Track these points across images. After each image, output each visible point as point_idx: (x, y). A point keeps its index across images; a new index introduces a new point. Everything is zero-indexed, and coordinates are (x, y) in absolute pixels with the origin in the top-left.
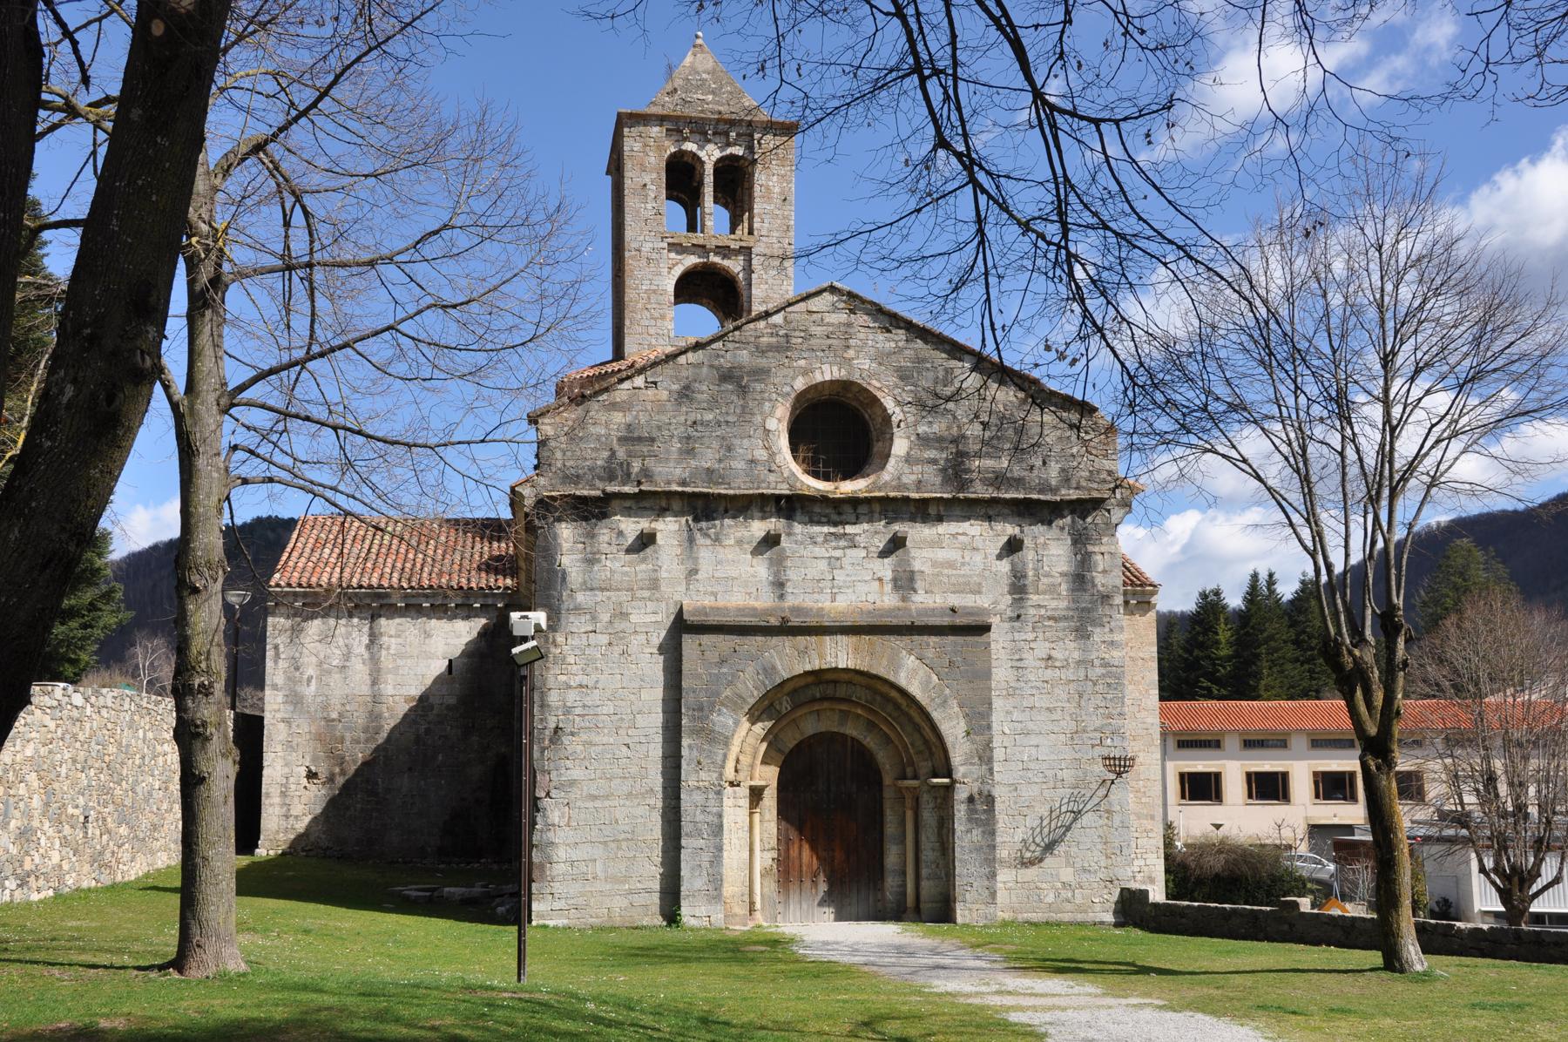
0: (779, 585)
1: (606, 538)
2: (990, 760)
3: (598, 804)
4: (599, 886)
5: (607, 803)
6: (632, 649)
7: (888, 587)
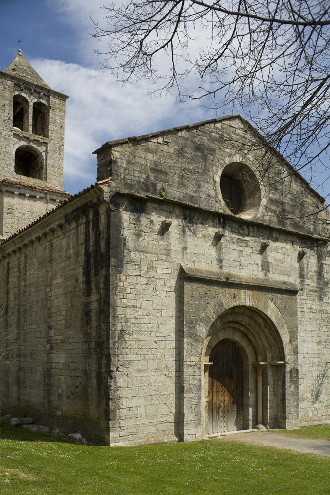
0: (220, 261)
1: (145, 224)
2: (298, 352)
3: (142, 374)
4: (144, 421)
5: (146, 374)
6: (158, 288)
7: (260, 269)
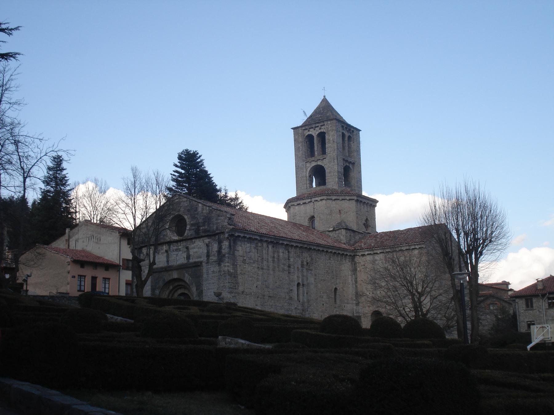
0: (168, 261)
